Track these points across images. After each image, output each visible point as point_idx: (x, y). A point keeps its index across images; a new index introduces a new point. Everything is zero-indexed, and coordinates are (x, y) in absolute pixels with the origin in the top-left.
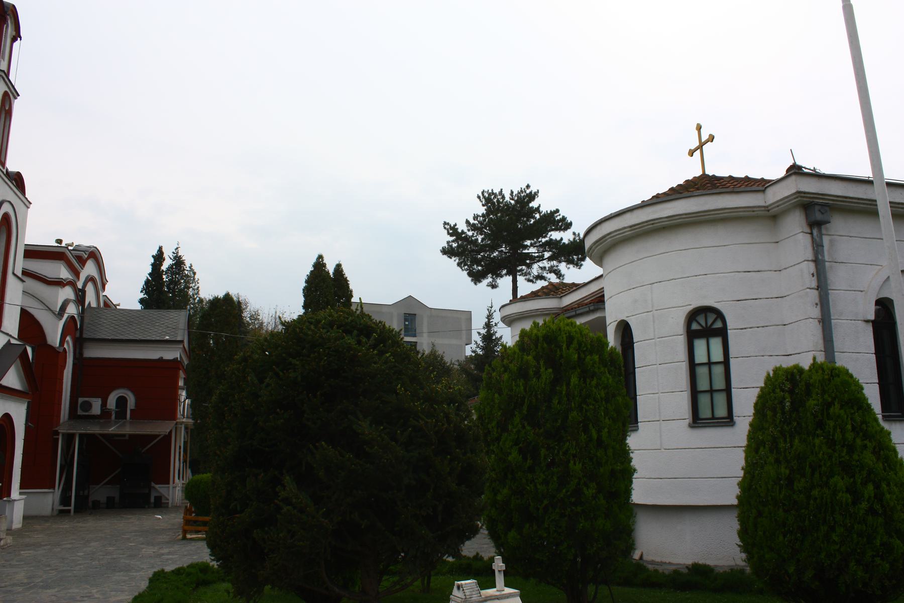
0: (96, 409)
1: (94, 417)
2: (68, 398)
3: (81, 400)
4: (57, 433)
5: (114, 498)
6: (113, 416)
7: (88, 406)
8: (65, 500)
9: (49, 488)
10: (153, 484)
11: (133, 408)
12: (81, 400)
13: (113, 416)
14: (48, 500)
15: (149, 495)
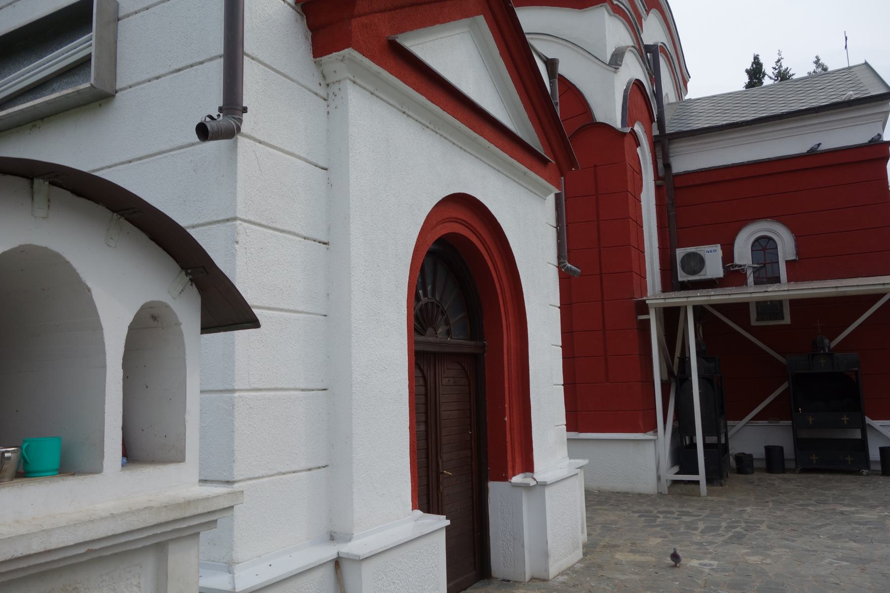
0: (714, 267)
1: (711, 284)
2: (656, 244)
3: (680, 253)
4: (643, 308)
5: (781, 449)
6: (751, 280)
7: (696, 263)
8: (683, 456)
9: (645, 431)
10: (868, 420)
11: (792, 257)
12: (680, 253)
13: (751, 280)
14: (641, 459)
15: (862, 445)
